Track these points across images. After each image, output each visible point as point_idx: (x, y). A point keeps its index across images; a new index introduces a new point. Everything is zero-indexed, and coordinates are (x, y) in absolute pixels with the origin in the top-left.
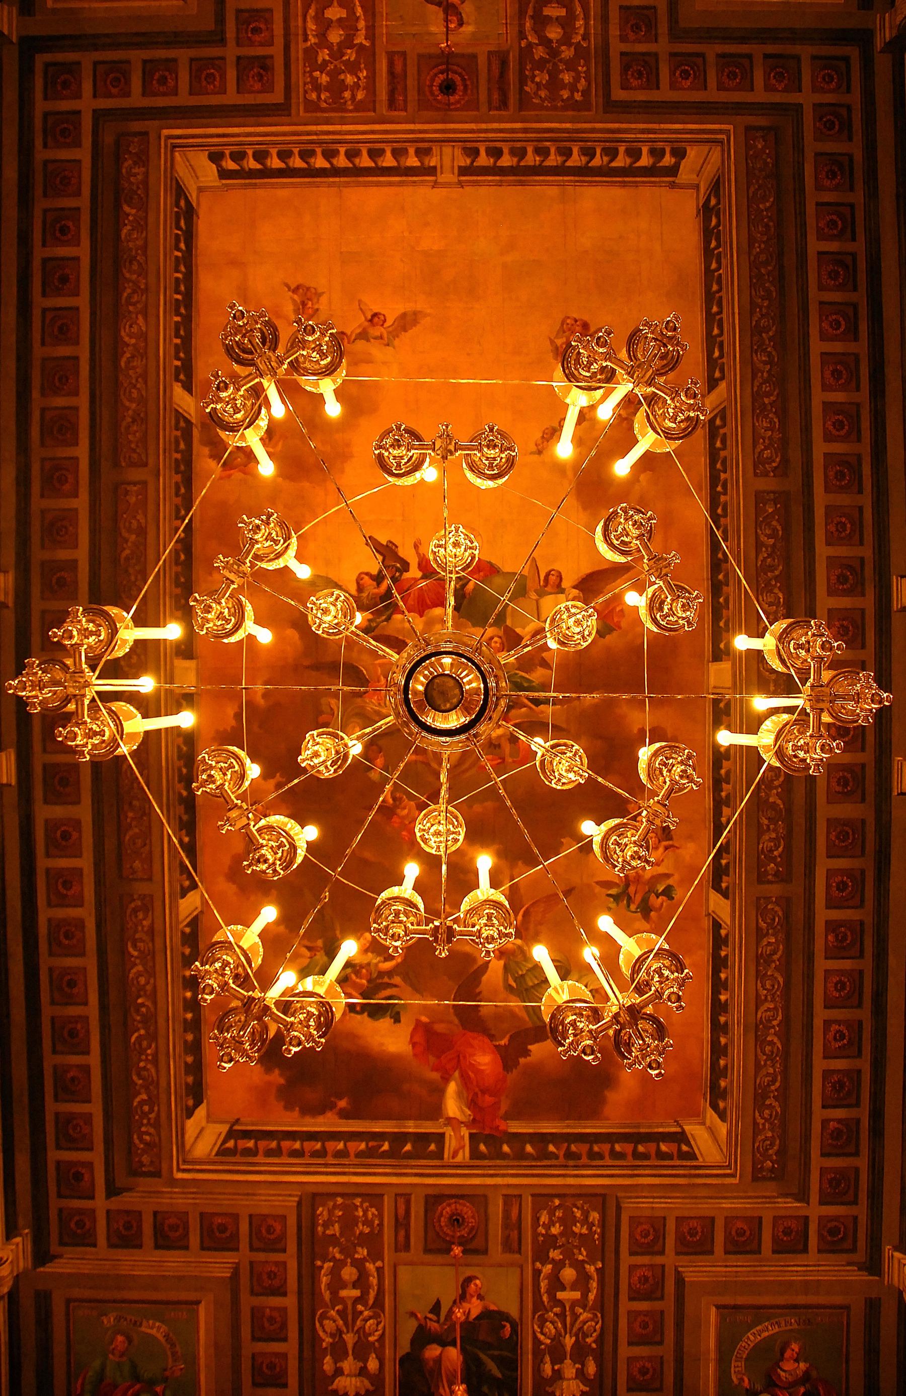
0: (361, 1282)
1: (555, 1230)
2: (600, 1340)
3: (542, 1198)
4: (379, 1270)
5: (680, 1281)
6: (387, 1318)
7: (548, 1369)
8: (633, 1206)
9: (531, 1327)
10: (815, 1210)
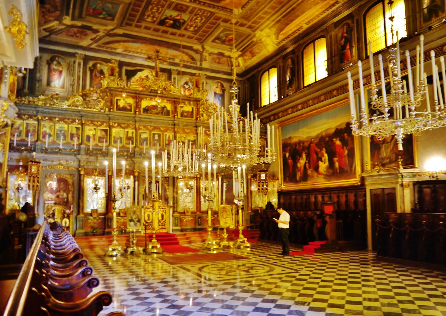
0: (158, 10)
1: (200, 13)
2: (200, 27)
3: (200, 9)
4: (162, 10)
5: (219, 24)
6: (160, 15)
7: (188, 27)
8: (216, 15)
9: (188, 22)
10: (250, 23)
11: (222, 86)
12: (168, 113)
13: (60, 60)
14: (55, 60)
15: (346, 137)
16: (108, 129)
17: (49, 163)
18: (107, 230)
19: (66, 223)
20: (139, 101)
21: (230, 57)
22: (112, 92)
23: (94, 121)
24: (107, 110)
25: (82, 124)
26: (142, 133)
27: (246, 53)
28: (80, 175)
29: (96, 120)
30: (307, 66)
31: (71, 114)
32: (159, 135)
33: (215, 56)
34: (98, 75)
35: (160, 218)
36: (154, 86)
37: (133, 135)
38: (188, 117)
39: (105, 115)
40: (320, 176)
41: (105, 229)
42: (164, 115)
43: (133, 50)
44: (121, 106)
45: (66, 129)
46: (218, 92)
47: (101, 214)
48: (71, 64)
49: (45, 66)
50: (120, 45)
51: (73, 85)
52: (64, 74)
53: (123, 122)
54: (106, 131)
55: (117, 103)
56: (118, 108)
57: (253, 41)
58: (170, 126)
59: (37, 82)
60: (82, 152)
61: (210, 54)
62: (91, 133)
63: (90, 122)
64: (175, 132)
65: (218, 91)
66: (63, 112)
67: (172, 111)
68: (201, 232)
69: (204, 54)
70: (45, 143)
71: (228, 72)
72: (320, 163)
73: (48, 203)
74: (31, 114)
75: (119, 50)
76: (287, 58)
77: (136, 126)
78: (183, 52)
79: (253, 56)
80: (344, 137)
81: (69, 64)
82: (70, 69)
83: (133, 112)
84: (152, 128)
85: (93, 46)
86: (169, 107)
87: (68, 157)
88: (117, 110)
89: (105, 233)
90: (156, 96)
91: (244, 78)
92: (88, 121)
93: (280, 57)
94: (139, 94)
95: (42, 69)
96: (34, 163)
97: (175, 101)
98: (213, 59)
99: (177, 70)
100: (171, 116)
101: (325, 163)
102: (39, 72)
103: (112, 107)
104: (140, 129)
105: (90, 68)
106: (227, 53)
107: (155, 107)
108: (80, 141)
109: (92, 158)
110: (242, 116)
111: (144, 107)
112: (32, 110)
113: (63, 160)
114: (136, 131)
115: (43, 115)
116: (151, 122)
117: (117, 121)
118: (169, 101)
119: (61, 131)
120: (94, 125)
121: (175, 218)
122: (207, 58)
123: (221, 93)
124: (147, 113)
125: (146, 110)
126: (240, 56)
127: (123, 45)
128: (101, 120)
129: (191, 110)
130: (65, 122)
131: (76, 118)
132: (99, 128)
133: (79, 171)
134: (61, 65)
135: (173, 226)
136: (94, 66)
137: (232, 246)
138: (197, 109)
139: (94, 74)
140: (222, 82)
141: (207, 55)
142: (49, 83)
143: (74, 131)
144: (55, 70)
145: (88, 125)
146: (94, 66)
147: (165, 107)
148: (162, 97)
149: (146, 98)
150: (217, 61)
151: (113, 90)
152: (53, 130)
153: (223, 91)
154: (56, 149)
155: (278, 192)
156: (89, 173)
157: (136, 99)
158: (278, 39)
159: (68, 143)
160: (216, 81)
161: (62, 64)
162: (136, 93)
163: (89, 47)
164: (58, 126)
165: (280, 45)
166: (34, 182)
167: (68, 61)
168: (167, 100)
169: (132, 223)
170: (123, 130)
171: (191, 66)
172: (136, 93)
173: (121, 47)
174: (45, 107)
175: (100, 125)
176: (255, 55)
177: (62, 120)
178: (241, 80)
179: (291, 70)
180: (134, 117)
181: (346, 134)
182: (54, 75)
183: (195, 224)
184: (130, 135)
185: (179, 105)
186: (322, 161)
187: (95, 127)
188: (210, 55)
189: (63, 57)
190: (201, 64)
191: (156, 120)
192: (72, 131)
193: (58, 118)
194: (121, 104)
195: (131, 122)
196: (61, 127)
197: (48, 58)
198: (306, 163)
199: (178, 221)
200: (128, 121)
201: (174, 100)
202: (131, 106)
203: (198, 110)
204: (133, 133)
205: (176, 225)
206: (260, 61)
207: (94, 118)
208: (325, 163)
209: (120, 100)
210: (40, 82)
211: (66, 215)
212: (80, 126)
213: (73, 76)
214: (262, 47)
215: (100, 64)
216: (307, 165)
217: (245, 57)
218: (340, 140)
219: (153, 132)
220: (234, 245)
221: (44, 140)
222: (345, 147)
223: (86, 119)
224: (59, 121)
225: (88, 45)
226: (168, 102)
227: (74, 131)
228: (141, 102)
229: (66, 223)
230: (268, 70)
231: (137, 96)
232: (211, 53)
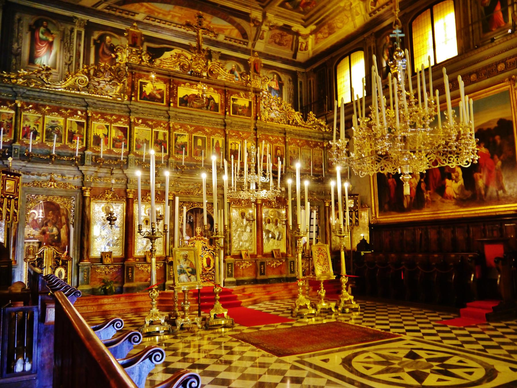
11: (279, 79)
12: (215, 108)
13: (50, 27)
14: (42, 25)
15: (499, 141)
16: (128, 127)
17: (35, 177)
18: (126, 285)
19: (60, 274)
20: (174, 87)
21: (297, 34)
22: (134, 71)
23: (107, 114)
24: (126, 97)
25: (87, 118)
26: (178, 135)
27: (322, 28)
28: (84, 198)
29: (110, 112)
30: (419, 43)
31: (69, 100)
32: (203, 140)
33: (278, 31)
34: (107, 52)
35: (205, 265)
36: (196, 67)
37: (165, 138)
38: (244, 115)
39: (123, 106)
40: (448, 201)
41: (123, 283)
42: (211, 110)
43: (160, 16)
44: (148, 94)
45: (62, 124)
46: (273, 87)
47: (116, 260)
48: (66, 33)
49: (27, 33)
50: (142, 6)
51: (69, 65)
52: (55, 48)
53: (151, 118)
54: (124, 130)
55: (141, 88)
56: (144, 97)
57: (340, 7)
58: (219, 127)
59: (13, 57)
60: (87, 162)
61: (272, 27)
62: (101, 133)
64: (225, 136)
65: (274, 85)
66: (58, 97)
67: (221, 105)
68: (264, 285)
69: (264, 27)
70: (28, 145)
71: (288, 60)
72: (448, 182)
73: (29, 243)
74: (5, 97)
75: (139, 17)
76: (384, 34)
77: (169, 124)
78: (232, 22)
79: (330, 34)
80: (495, 142)
81: (63, 32)
82: (65, 40)
83: (165, 104)
84: (193, 128)
85: (100, 8)
86: (217, 98)
87: (66, 169)
88: (140, 99)
89: (124, 289)
90: (198, 81)
91: (308, 70)
92: (97, 114)
93: (371, 34)
94: (174, 77)
95: (21, 37)
96: (9, 176)
97: (226, 90)
98: (273, 37)
99: (219, 52)
100: (220, 112)
101: (456, 182)
102: (17, 41)
103: (133, 95)
104: (175, 130)
105: (95, 41)
106: (296, 27)
107: (196, 97)
108: (84, 145)
109: (103, 172)
110: (316, 117)
111: (182, 97)
112: (5, 91)
113: (56, 173)
114: (170, 132)
115: (25, 100)
116: (191, 119)
117: (141, 116)
118: (217, 89)
119: (53, 127)
120: (106, 120)
121: (228, 264)
122: (265, 35)
123: (278, 88)
124: (186, 106)
125: (185, 101)
126: (313, 32)
127: (147, 8)
128: (117, 113)
129: (247, 105)
130: (61, 114)
131: (78, 108)
132: (113, 125)
133: (82, 192)
134: (52, 34)
135: (225, 277)
136: (102, 38)
137: (334, 310)
138: (256, 103)
139: (101, 50)
140: (279, 73)
141: (267, 28)
142: (32, 59)
143: (75, 129)
144: (41, 40)
145: (97, 120)
146: (102, 38)
147: (213, 99)
148: (209, 84)
149: (184, 83)
150: (277, 40)
151: (135, 69)
152: (41, 126)
153: (281, 85)
154: (46, 155)
155: (370, 225)
156: (98, 195)
157: (170, 84)
158: (375, 5)
159: (65, 147)
160: (271, 71)
161: (52, 32)
162: (169, 76)
163: (94, 8)
164: (48, 119)
165: (374, 16)
166: (9, 206)
167: (62, 28)
168: (215, 89)
169: (183, 277)
170: (150, 129)
171: (239, 48)
172: (169, 76)
173: (143, 10)
174: (29, 88)
175: (116, 121)
176: (335, 32)
177: (57, 110)
178: (303, 73)
179: (389, 52)
180: (167, 111)
181: (497, 137)
182: (40, 48)
183: (256, 273)
184: (161, 138)
185: (232, 97)
186: (450, 178)
187: (108, 124)
188: (270, 29)
189: (54, 21)
190: (253, 45)
191: (198, 117)
192: (71, 128)
193: (49, 106)
194: (148, 89)
195: (162, 119)
196: (53, 121)
197: (32, 22)
198: (420, 183)
199: (232, 268)
200: (158, 116)
201: (224, 88)
202: (162, 94)
203: (257, 105)
204: (164, 135)
205: (230, 276)
206: (338, 42)
207: (105, 109)
208: (456, 182)
209: (145, 84)
210: (18, 57)
211: (61, 263)
212: (84, 121)
213: (69, 51)
214: (348, 17)
215: (111, 36)
216: (423, 185)
217: (320, 35)
218: (485, 147)
219: (193, 135)
220: (336, 307)
221: (25, 141)
222: (496, 157)
223: (94, 110)
224: (50, 112)
225: (93, 6)
226: (216, 91)
227: (75, 129)
228: (177, 90)
229: (60, 274)
230: (349, 54)
231: (172, 80)
232: (272, 26)
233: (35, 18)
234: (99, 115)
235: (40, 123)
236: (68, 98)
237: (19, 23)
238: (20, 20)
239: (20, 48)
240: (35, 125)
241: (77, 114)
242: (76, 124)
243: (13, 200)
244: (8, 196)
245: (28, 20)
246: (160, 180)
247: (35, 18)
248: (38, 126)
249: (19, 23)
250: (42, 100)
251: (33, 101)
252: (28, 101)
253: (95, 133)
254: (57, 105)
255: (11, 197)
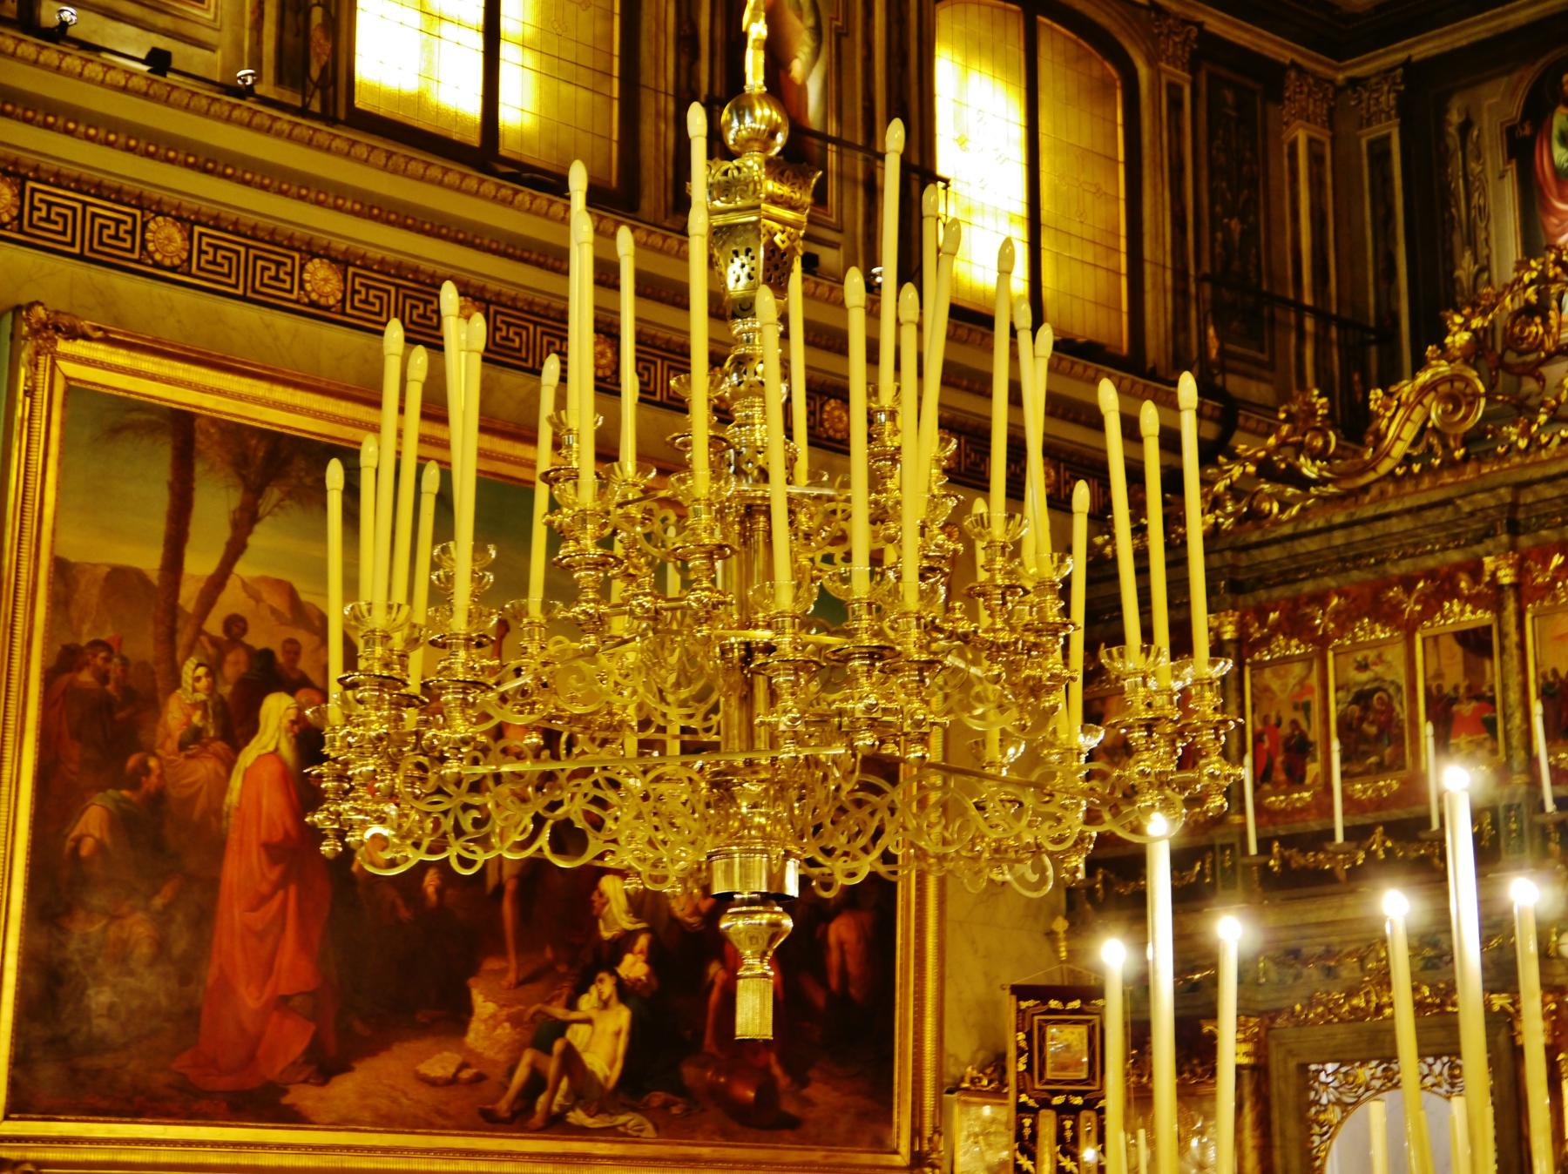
25: (1493, 598)
63: (1557, 560)
95: (1482, 210)
96: (1054, 1004)
102: (1471, 242)
115: (1249, 600)
119: (1362, 698)
130: (1388, 614)
192: (1439, 675)
193: (1341, 593)
197: (1514, 109)
212: (1484, 617)
224: (1345, 620)
233: (1525, 77)
234: (1557, 560)
235: (1311, 690)
236: (1396, 525)
237: (1463, 147)
238: (1465, 127)
239: (1486, 268)
240: (1296, 707)
241: (1454, 593)
242: (1458, 650)
243: (1085, 1114)
244: (1058, 1100)
245: (1496, 104)
246: (1195, 964)
247: (1525, 77)
248: (1306, 708)
249: (1463, 147)
250: (1313, 576)
251: (1277, 593)
252: (1262, 595)
253: (1548, 669)
254: (1369, 576)
255: (1078, 1101)
